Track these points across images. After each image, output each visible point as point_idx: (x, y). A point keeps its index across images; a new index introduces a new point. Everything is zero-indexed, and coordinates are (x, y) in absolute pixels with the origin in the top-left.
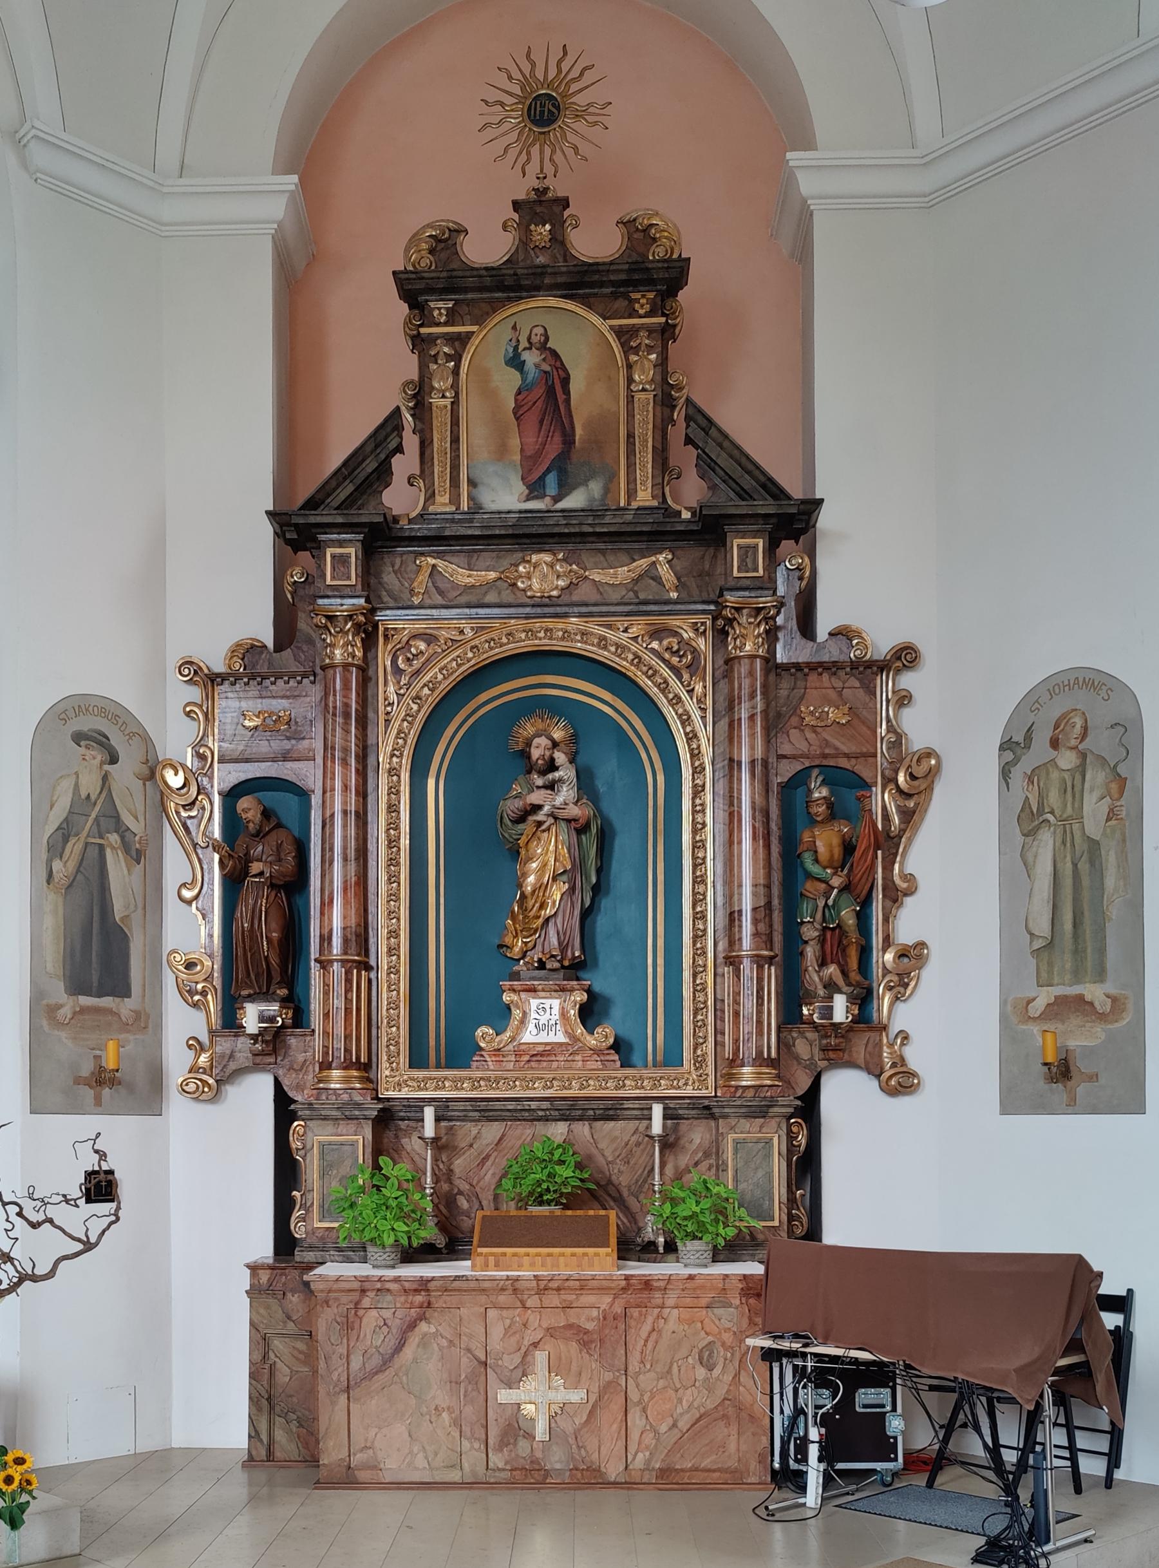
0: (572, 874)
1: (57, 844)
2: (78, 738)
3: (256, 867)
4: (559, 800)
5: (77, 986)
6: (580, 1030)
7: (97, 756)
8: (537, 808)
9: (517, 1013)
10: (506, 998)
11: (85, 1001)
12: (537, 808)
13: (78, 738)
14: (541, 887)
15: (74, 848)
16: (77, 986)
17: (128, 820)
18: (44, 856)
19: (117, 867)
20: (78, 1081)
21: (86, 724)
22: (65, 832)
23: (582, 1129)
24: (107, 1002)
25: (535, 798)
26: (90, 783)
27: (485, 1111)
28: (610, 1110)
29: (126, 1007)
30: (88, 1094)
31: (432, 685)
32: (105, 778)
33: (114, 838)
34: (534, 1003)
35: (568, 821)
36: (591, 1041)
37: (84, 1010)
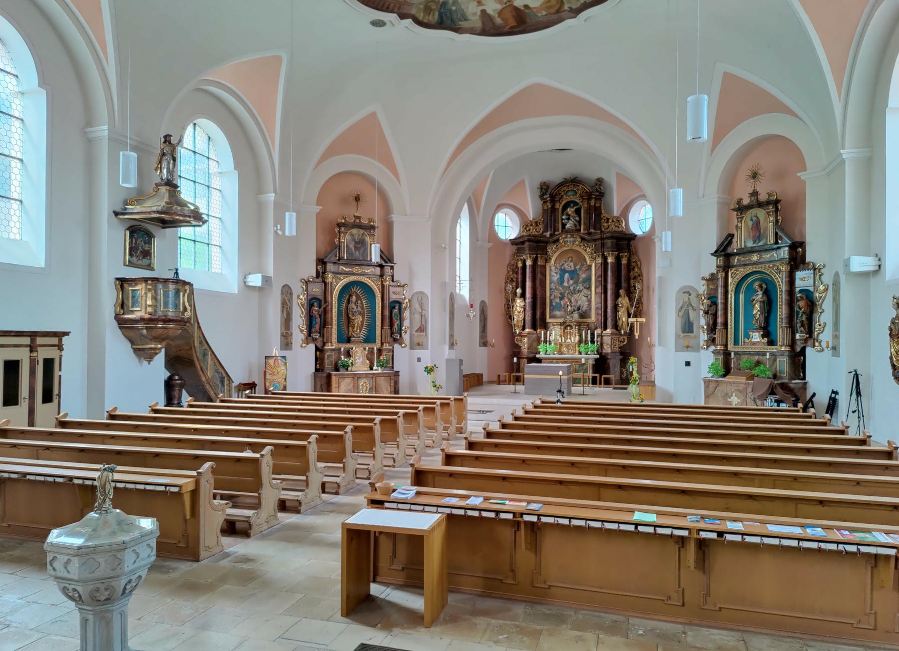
0: (762, 310)
1: (680, 310)
2: (684, 293)
3: (710, 312)
4: (758, 298)
5: (684, 332)
6: (761, 339)
7: (687, 295)
8: (754, 299)
9: (751, 336)
10: (750, 333)
11: (685, 334)
12: (754, 299)
13: (684, 293)
14: (756, 314)
15: (683, 311)
16: (684, 332)
17: (693, 304)
18: (678, 312)
19: (691, 312)
20: (684, 347)
21: (685, 291)
22: (681, 308)
23: (761, 357)
24: (689, 334)
25: (754, 298)
26: (686, 300)
27: (745, 353)
28: (764, 354)
29: (692, 335)
30: (686, 349)
31: (737, 279)
32: (689, 298)
33: (690, 308)
34: (754, 334)
35: (761, 301)
36: (763, 341)
37: (685, 336)
